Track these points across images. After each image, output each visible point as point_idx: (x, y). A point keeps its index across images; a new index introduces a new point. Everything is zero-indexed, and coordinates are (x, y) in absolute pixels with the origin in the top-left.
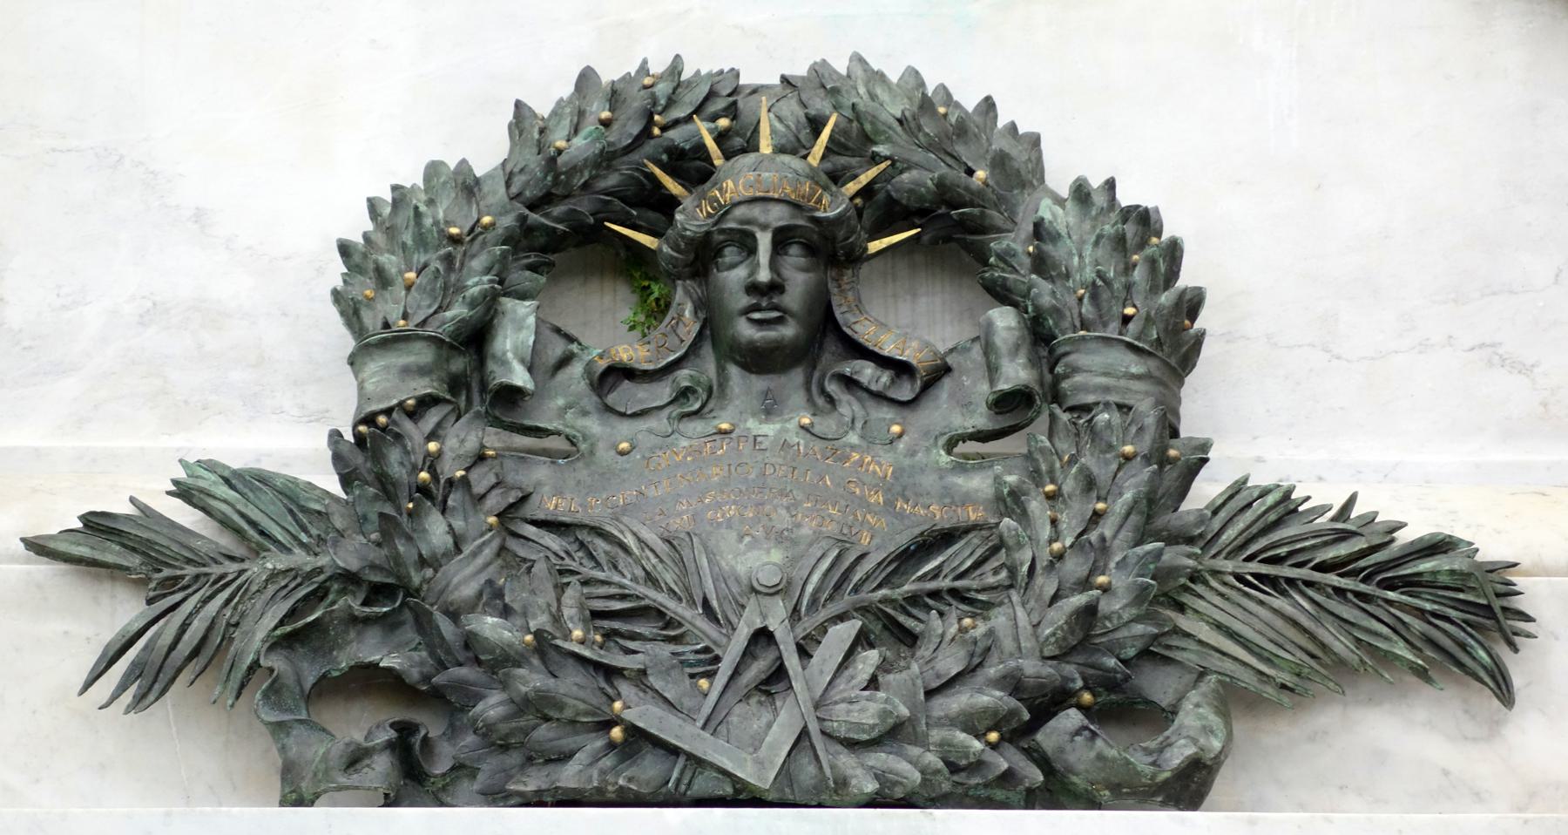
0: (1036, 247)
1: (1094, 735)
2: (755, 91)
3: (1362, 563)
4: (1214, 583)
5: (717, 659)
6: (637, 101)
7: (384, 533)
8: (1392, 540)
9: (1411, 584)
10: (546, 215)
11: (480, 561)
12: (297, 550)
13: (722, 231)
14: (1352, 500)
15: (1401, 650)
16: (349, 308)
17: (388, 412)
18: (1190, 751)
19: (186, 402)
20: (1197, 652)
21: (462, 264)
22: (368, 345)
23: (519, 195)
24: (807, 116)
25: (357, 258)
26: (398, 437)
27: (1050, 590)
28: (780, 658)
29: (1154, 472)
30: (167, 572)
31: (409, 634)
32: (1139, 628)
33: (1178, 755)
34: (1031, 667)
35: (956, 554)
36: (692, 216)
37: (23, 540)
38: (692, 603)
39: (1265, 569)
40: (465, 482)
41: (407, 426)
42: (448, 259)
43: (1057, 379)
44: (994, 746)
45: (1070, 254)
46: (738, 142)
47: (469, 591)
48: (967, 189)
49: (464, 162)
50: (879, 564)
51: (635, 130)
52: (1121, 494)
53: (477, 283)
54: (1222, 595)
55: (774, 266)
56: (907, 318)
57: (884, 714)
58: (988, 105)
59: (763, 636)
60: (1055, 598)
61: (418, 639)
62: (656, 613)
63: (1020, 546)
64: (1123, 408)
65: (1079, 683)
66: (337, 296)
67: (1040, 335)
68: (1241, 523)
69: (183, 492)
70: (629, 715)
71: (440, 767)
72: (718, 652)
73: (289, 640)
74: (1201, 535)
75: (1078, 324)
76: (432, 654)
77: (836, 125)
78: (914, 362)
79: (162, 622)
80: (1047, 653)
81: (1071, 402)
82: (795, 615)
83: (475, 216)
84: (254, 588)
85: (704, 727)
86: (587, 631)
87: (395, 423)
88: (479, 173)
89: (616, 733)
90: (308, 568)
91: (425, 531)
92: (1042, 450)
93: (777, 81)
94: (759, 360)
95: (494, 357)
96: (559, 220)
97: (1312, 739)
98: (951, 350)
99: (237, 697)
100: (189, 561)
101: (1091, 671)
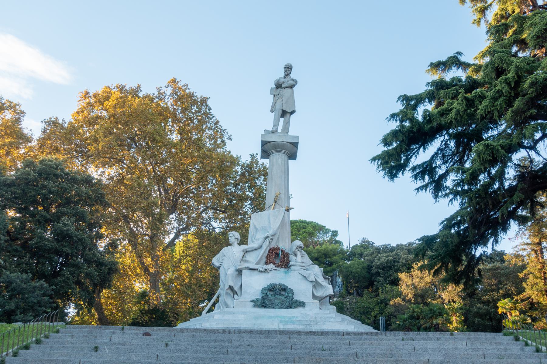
56: (283, 293)
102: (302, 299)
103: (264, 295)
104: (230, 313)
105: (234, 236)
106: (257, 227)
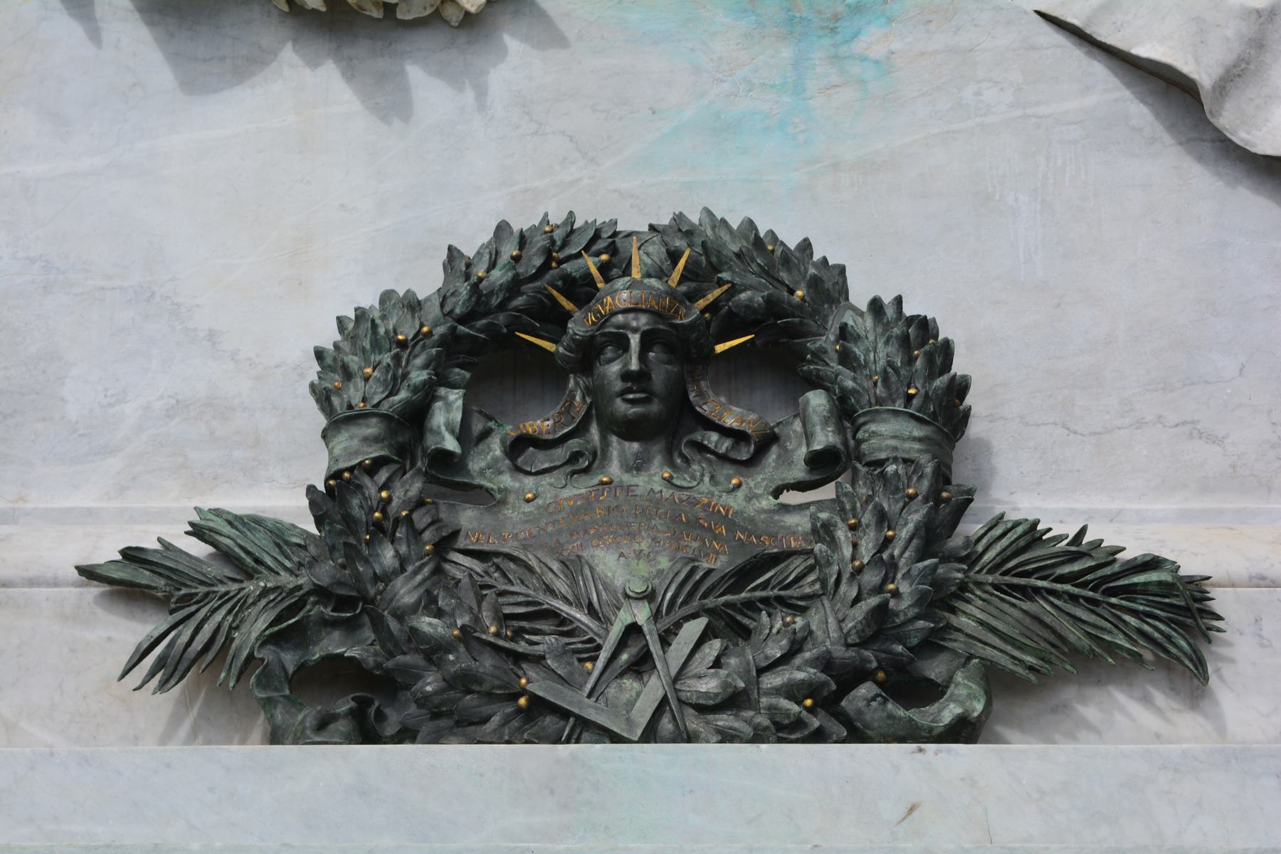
0: (842, 346)
1: (886, 700)
2: (630, 235)
3: (1089, 577)
4: (978, 593)
5: (599, 647)
6: (540, 242)
7: (346, 556)
8: (1114, 561)
9: (1130, 591)
10: (471, 328)
11: (419, 578)
12: (282, 573)
13: (603, 335)
14: (1083, 531)
15: (1121, 641)
16: (323, 397)
17: (351, 469)
18: (959, 710)
19: (201, 474)
20: (965, 643)
21: (408, 362)
22: (336, 422)
23: (451, 312)
24: (668, 251)
25: (329, 361)
26: (359, 488)
27: (854, 593)
28: (647, 645)
29: (931, 508)
30: (184, 591)
31: (369, 634)
32: (921, 624)
33: (948, 712)
34: (839, 652)
35: (781, 572)
36: (579, 326)
37: (77, 568)
38: (579, 606)
39: (1016, 581)
40: (409, 519)
41: (366, 480)
42: (397, 358)
43: (859, 442)
44: (810, 710)
45: (868, 350)
46: (615, 265)
47: (409, 599)
48: (790, 304)
49: (408, 291)
50: (723, 578)
51: (538, 262)
52: (906, 524)
53: (419, 376)
54: (984, 600)
55: (642, 357)
57: (725, 685)
58: (806, 246)
59: (633, 630)
60: (857, 600)
61: (373, 637)
62: (552, 614)
63: (829, 564)
64: (906, 461)
65: (874, 665)
66: (312, 386)
68: (998, 547)
69: (197, 531)
70: (530, 687)
71: (390, 730)
72: (599, 641)
73: (275, 639)
74: (968, 556)
75: (873, 401)
76: (383, 647)
77: (689, 257)
78: (749, 431)
79: (180, 628)
80: (850, 641)
81: (869, 459)
82: (656, 616)
83: (418, 327)
84: (250, 601)
85: (589, 696)
86: (500, 627)
87: (356, 477)
88: (421, 297)
89: (522, 701)
90: (291, 586)
91: (378, 555)
92: (846, 494)
93: (646, 229)
94: (629, 430)
95: (431, 430)
96: (479, 331)
97: (1054, 710)
98: (778, 424)
99: (238, 681)
100: (202, 583)
101: (884, 655)
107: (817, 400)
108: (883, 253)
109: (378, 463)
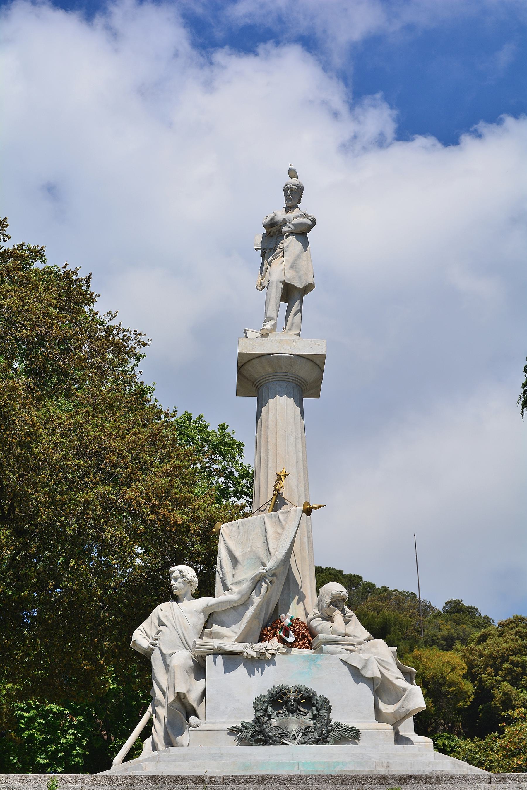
16: (254, 708)
59: (294, 735)
62: (284, 733)
67: (317, 710)
69: (241, 724)
102: (351, 723)
103: (259, 714)
104: (184, 758)
105: (184, 574)
106: (238, 554)
107: (314, 708)
108: (321, 691)
109: (262, 716)
